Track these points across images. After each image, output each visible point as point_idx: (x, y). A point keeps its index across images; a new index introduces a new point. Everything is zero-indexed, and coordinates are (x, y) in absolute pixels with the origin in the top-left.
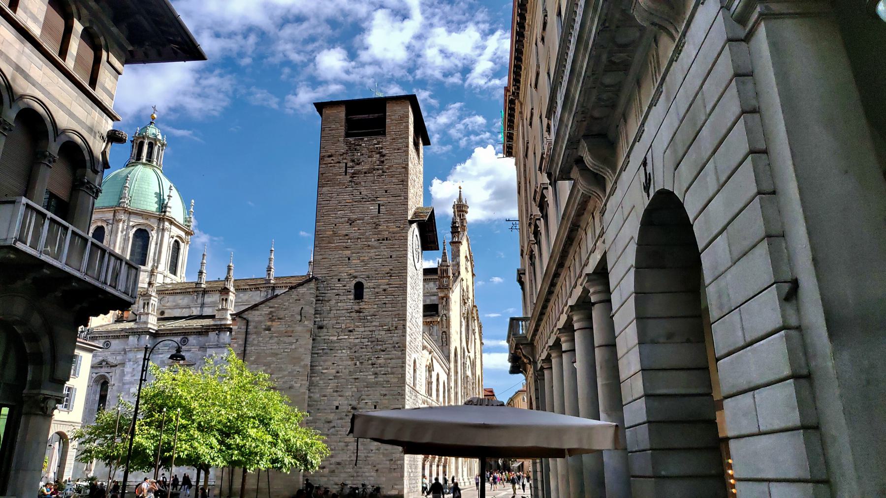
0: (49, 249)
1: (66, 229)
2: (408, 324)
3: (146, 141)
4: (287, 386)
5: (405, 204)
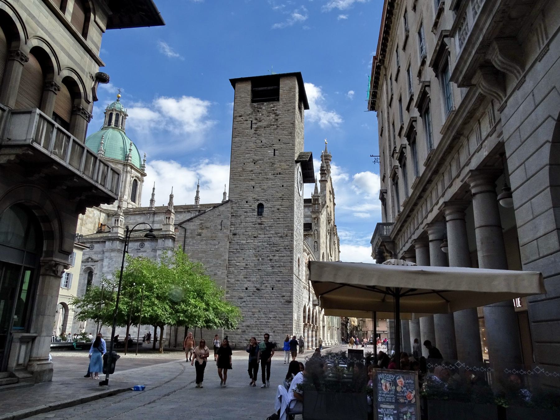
0: (57, 151)
1: (69, 137)
2: (295, 233)
3: (114, 113)
4: (213, 273)
5: (293, 149)
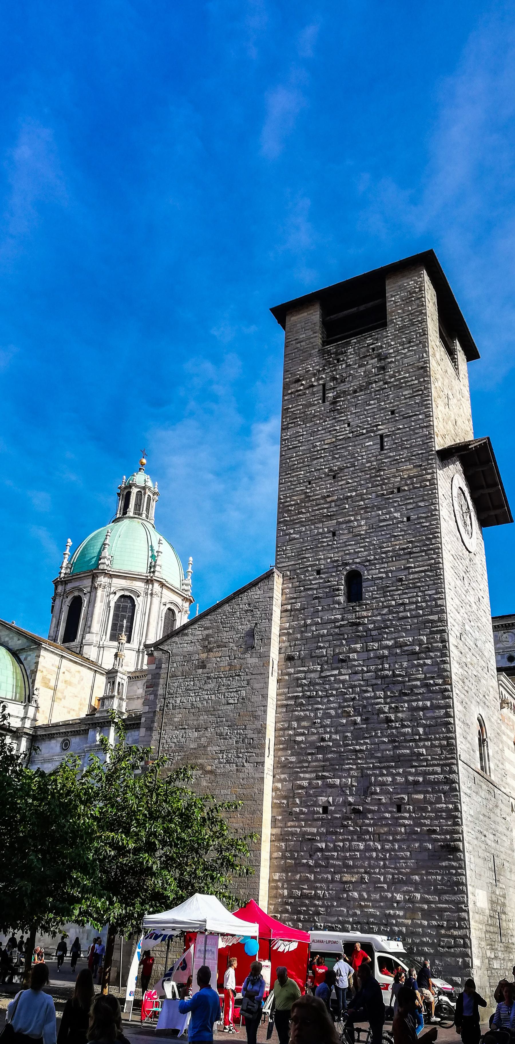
3: (134, 491)
